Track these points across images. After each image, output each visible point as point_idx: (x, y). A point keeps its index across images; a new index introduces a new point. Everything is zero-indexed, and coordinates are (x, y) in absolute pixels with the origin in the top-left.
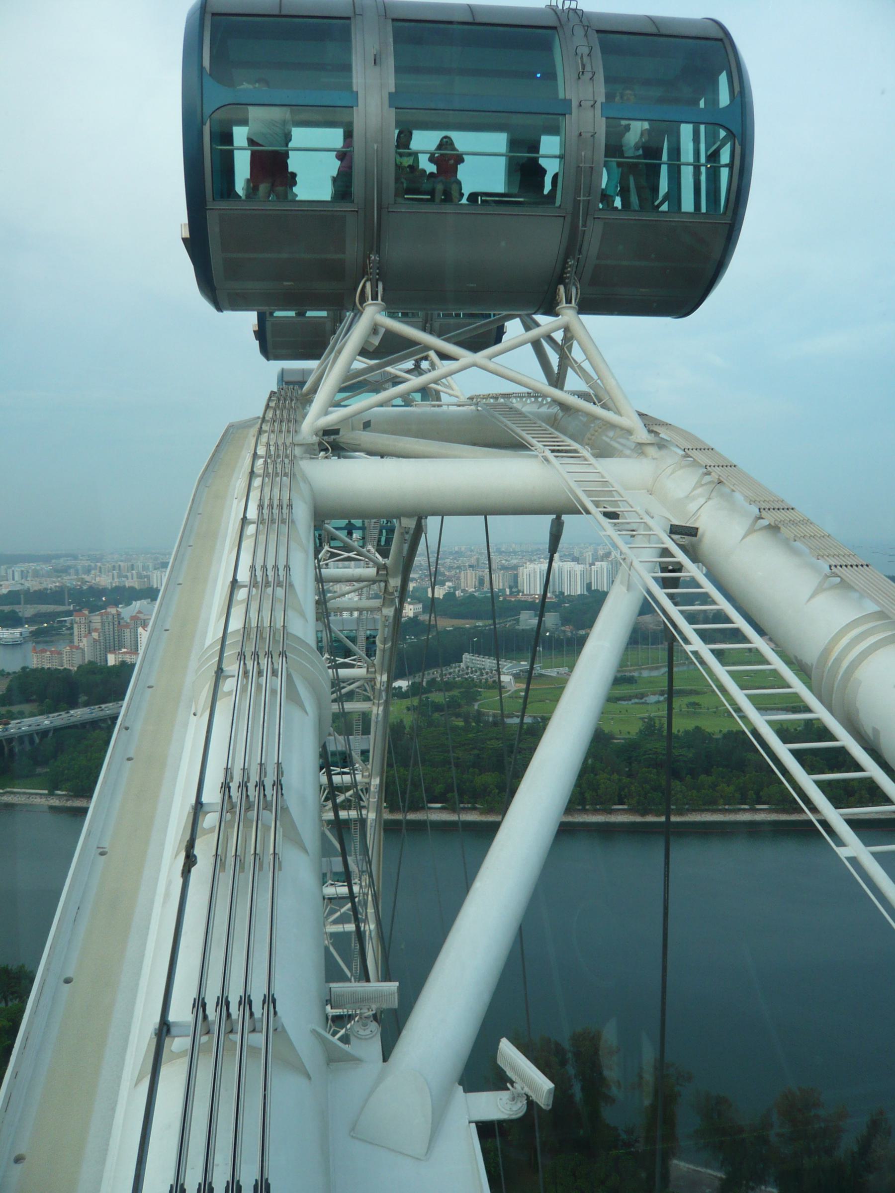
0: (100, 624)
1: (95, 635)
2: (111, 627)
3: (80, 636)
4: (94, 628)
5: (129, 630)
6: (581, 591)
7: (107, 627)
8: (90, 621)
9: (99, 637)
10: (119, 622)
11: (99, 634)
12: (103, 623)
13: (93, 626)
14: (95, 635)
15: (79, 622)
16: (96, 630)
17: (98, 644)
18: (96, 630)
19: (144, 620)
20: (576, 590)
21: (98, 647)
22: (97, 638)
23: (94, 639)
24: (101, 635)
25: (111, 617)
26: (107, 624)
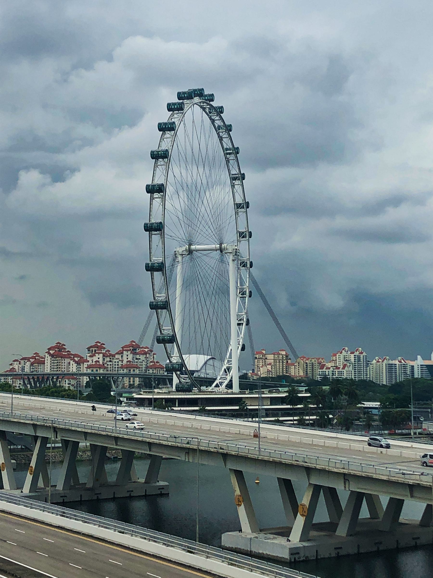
0: (273, 361)
1: (269, 367)
4: (268, 363)
5: (293, 367)
7: (278, 364)
8: (266, 359)
9: (272, 369)
10: (287, 361)
11: (272, 367)
15: (258, 358)
17: (270, 373)
18: (270, 364)
22: (270, 369)
23: (268, 369)
24: (273, 367)
25: (281, 356)
26: (278, 361)
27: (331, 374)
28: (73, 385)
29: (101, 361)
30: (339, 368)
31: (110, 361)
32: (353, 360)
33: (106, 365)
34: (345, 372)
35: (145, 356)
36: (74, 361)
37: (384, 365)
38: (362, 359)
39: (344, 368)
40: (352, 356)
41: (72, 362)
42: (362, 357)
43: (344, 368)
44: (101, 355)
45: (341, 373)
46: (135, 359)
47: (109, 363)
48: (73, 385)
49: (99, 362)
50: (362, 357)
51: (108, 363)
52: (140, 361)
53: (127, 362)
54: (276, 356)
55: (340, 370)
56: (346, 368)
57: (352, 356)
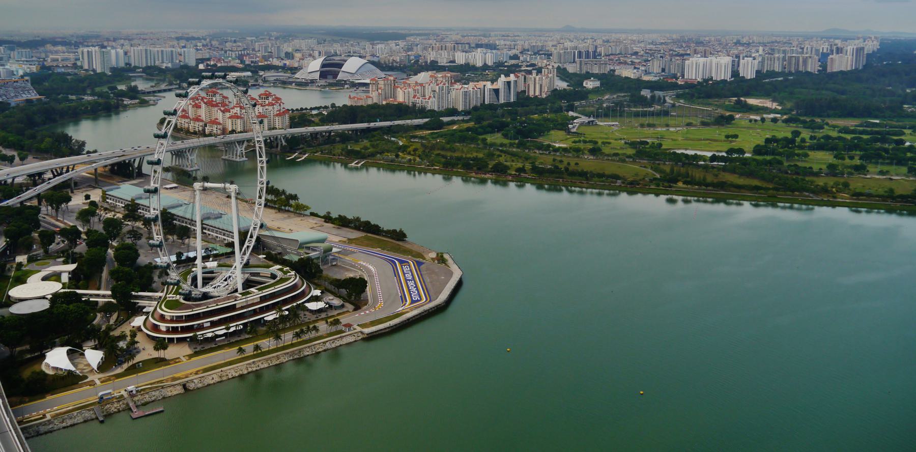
3: (372, 91)
6: (751, 77)
7: (387, 87)
12: (385, 85)
13: (379, 86)
14: (380, 91)
16: (380, 88)
19: (409, 84)
20: (747, 75)
25: (389, 81)
27: (420, 102)
28: (219, 129)
29: (238, 112)
30: (426, 99)
31: (246, 112)
32: (437, 91)
33: (242, 116)
35: (272, 107)
36: (220, 110)
37: (461, 92)
38: (445, 88)
39: (429, 99)
40: (437, 87)
41: (219, 110)
42: (444, 87)
43: (429, 99)
44: (238, 109)
45: (427, 103)
46: (264, 110)
47: (244, 114)
48: (219, 129)
49: (237, 113)
50: (444, 87)
51: (244, 114)
52: (268, 111)
53: (259, 113)
54: (386, 82)
55: (427, 100)
57: (437, 87)
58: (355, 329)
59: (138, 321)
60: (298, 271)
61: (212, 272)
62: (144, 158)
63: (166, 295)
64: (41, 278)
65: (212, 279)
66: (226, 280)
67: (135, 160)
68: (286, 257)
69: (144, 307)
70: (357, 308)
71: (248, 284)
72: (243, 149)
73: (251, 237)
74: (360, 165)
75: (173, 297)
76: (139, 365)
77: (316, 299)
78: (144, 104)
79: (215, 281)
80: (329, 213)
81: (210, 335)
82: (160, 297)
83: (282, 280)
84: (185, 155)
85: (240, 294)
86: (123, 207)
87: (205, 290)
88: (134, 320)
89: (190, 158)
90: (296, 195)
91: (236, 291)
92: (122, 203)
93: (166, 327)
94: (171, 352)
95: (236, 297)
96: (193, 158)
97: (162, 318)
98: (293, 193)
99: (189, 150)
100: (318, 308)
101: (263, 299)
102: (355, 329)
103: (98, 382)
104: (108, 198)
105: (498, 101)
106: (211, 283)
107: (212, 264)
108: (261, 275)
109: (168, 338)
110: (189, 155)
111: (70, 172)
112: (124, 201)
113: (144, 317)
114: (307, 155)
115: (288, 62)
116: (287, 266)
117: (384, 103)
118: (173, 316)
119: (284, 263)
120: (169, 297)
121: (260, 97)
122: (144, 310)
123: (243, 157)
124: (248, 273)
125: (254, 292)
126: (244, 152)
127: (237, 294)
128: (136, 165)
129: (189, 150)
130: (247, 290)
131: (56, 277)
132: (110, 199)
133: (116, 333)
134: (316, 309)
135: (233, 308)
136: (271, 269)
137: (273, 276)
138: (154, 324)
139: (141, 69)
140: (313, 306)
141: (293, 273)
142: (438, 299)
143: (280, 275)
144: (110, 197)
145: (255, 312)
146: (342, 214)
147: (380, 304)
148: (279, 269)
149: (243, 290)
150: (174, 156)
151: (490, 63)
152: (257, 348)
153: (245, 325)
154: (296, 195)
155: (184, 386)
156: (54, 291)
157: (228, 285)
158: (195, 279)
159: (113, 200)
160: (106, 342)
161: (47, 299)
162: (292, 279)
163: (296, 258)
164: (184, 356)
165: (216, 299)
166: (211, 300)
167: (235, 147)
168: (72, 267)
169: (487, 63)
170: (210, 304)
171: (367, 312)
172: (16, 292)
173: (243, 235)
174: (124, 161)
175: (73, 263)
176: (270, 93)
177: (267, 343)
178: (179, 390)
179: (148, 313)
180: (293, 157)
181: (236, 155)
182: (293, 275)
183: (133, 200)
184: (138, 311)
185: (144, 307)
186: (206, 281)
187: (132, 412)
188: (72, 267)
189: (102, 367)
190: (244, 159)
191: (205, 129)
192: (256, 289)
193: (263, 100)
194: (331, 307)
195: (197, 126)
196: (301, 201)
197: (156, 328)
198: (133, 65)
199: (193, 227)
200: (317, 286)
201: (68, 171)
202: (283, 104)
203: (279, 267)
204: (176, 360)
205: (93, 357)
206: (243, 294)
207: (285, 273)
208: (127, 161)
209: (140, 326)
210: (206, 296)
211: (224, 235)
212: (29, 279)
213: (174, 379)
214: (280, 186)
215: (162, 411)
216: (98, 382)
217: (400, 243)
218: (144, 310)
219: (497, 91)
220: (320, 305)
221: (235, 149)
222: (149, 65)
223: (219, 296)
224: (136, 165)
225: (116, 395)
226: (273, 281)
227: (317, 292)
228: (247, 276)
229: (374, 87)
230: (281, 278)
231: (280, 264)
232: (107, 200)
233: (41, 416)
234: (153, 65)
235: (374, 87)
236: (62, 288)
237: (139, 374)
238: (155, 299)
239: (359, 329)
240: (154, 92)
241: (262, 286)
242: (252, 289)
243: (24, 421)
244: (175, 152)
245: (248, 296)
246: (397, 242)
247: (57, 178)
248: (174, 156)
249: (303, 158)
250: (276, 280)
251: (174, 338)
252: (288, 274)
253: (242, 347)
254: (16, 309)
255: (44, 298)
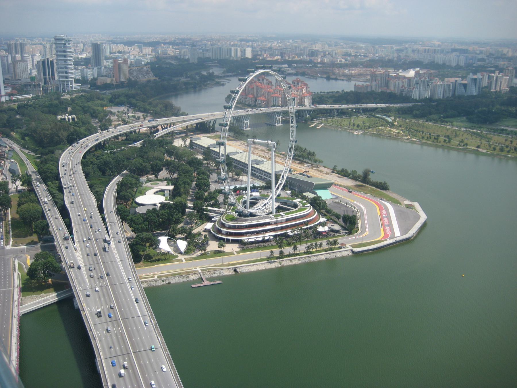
2: (385, 79)
14: (377, 81)
21: (378, 86)
34: (414, 91)
38: (425, 82)
39: (413, 89)
55: (411, 90)
56: (414, 89)
58: (348, 248)
59: (209, 226)
60: (311, 204)
61: (256, 199)
62: (216, 120)
63: (227, 210)
64: (153, 193)
65: (255, 204)
66: (265, 205)
67: (210, 121)
68: (305, 194)
69: (213, 217)
70: (350, 233)
71: (279, 209)
72: (280, 118)
73: (283, 177)
74: (359, 134)
75: (231, 213)
76: (208, 254)
77: (323, 224)
78: (218, 84)
79: (257, 205)
80: (335, 166)
81: (253, 240)
82: (223, 212)
83: (301, 210)
84: (242, 120)
85: (273, 215)
86: (202, 151)
87: (251, 210)
88: (206, 225)
89: (245, 122)
90: (314, 153)
91: (271, 213)
92: (202, 149)
93: (226, 231)
94: (228, 248)
95: (270, 217)
96: (247, 122)
97: (223, 225)
98: (312, 151)
99: (245, 116)
100: (324, 231)
101: (287, 220)
102: (348, 248)
103: (184, 261)
104: (193, 145)
105: (466, 92)
106: (255, 206)
107: (256, 194)
108: (288, 204)
109: (226, 239)
110: (244, 120)
111: (172, 127)
112: (203, 148)
113: (212, 224)
114: (323, 125)
115: (312, 58)
116: (305, 200)
117: (380, 91)
118: (230, 225)
119: (304, 198)
120: (229, 213)
121: (293, 82)
122: (213, 219)
123: (279, 123)
124: (279, 202)
125: (282, 216)
126: (280, 119)
127: (271, 216)
128: (211, 124)
129: (245, 116)
130: (278, 213)
131: (162, 192)
132: (195, 146)
133: (195, 231)
134: (322, 231)
135: (269, 224)
136: (294, 201)
137: (296, 206)
138: (218, 229)
139: (217, 61)
140: (320, 229)
141: (309, 205)
142: (407, 234)
143: (300, 205)
144: (194, 145)
145: (282, 228)
146: (345, 168)
147: (367, 233)
148: (299, 202)
149: (276, 212)
150: (235, 120)
151: (462, 64)
152: (281, 252)
153: (275, 236)
154: (314, 153)
155: (235, 270)
156: (160, 202)
157: (265, 208)
158: (245, 202)
159: (197, 147)
160: (189, 237)
161: (157, 206)
162: (308, 209)
163: (311, 196)
164: (235, 252)
165: (257, 217)
166: (255, 217)
167: (274, 116)
168: (171, 187)
169: (459, 64)
170: (253, 220)
171: (357, 237)
172: (140, 200)
173: (277, 177)
174: (204, 122)
175: (172, 185)
176: (300, 80)
177: (288, 250)
178: (231, 272)
179: (215, 221)
180: (313, 125)
181: (275, 122)
182: (308, 207)
183: (208, 148)
184: (209, 219)
185: (213, 217)
186: (253, 204)
187: (204, 281)
188: (171, 187)
189: (188, 252)
190: (280, 124)
191: (255, 103)
192: (284, 213)
193: (295, 85)
194: (332, 230)
195: (251, 101)
196: (317, 157)
197: (219, 232)
198: (212, 58)
199: (245, 168)
200: (324, 215)
201: (170, 126)
202: (309, 88)
203: (299, 200)
204: (231, 253)
205: (182, 245)
206: (275, 216)
207: (304, 204)
208: (206, 122)
209: (210, 229)
210: (252, 215)
211: (265, 175)
212: (147, 192)
213: (229, 265)
214: (303, 146)
215: (221, 283)
216: (184, 261)
217: (384, 192)
218: (213, 219)
219: (465, 86)
220: (326, 228)
221: (275, 117)
222: (222, 58)
223: (260, 216)
224: (211, 124)
225: (194, 270)
226: (295, 210)
227: (322, 220)
228: (278, 204)
229: (373, 79)
230: (301, 208)
231: (300, 198)
232: (193, 147)
233: (152, 276)
234: (224, 58)
235: (373, 79)
236: (166, 200)
237: (208, 259)
238: (219, 213)
239: (351, 248)
240: (224, 76)
241: (288, 211)
242: (281, 213)
243: (143, 277)
244: (235, 117)
245: (278, 217)
246: (382, 191)
247: (164, 130)
248: (235, 120)
249: (320, 127)
250: (297, 209)
251: (230, 239)
252: (305, 205)
253: (272, 250)
254: (139, 210)
255: (155, 205)
